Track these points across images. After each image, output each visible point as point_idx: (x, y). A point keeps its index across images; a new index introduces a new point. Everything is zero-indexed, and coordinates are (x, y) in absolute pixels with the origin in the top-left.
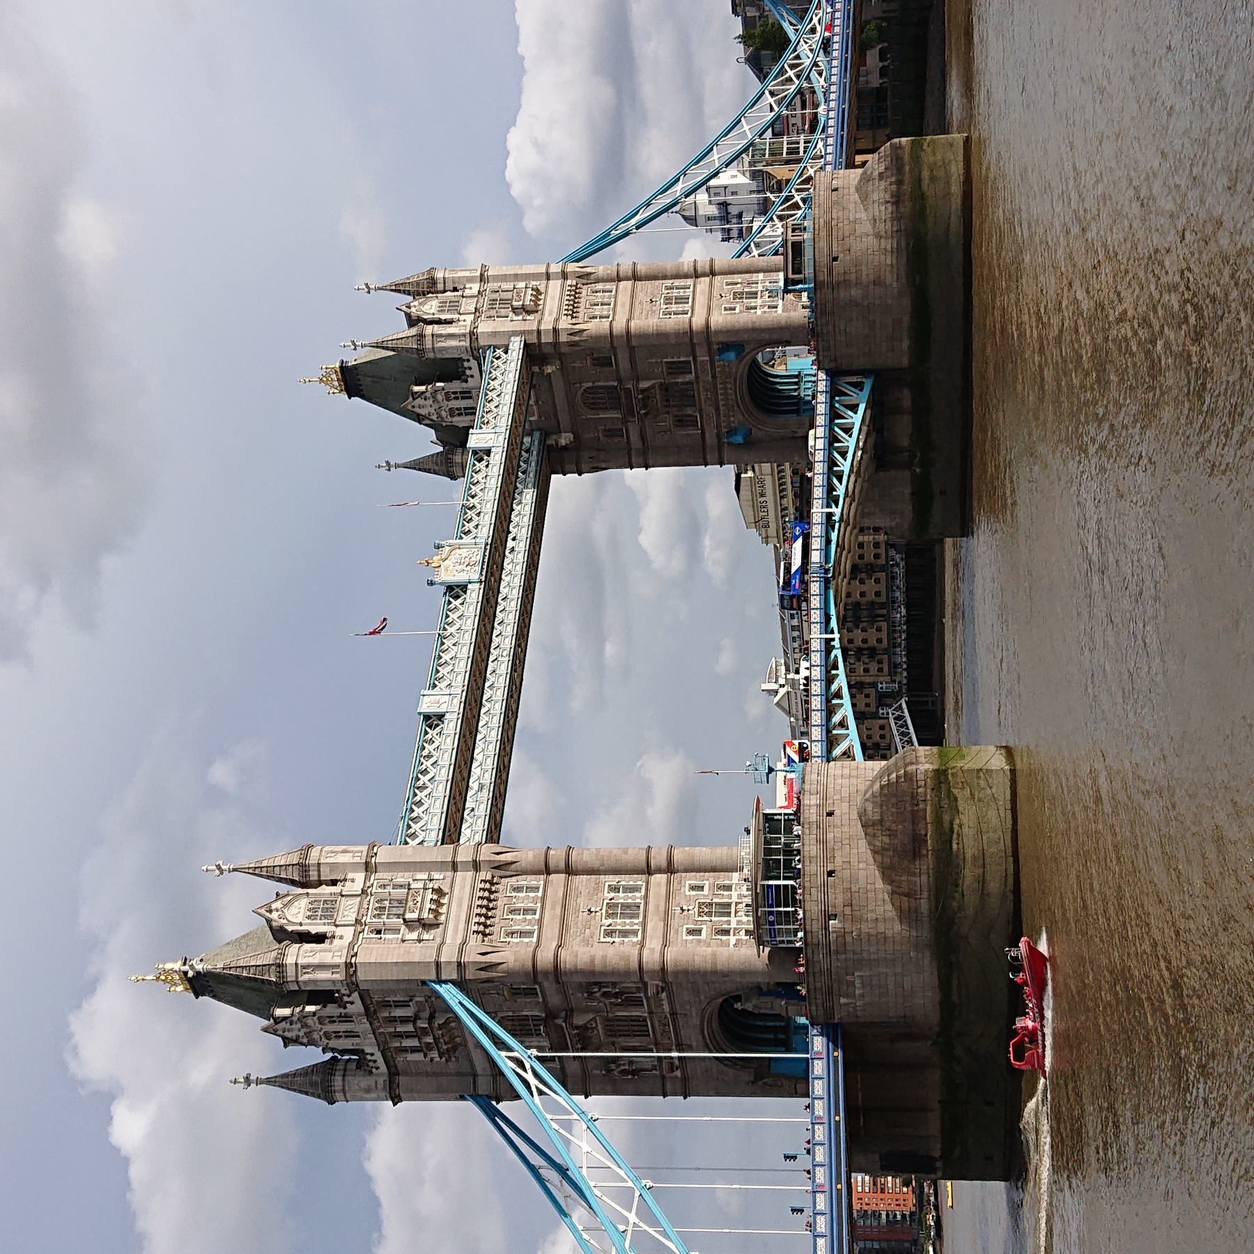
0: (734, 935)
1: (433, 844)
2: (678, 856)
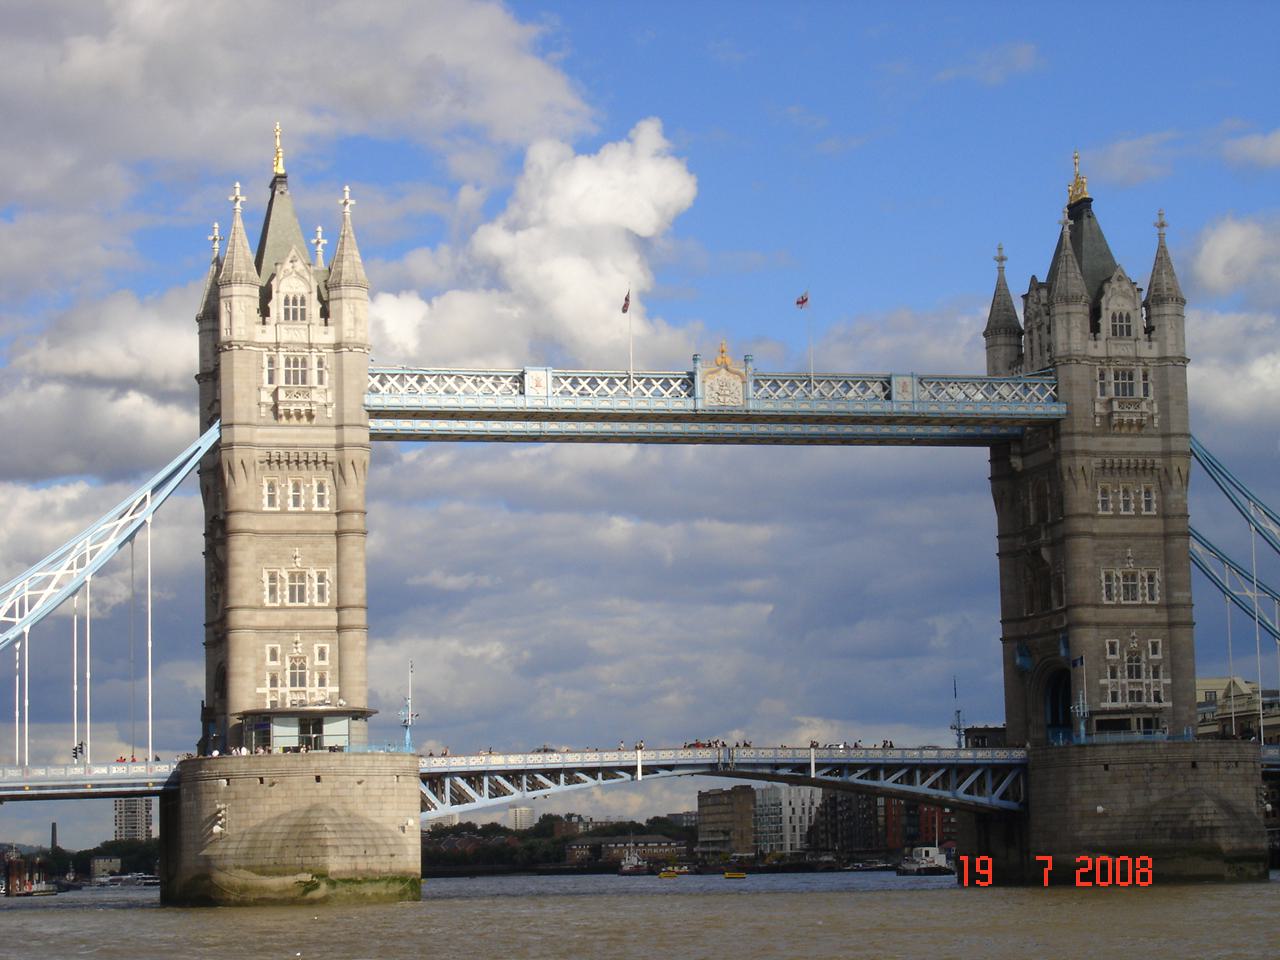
0: (271, 691)
1: (366, 402)
2: (350, 636)
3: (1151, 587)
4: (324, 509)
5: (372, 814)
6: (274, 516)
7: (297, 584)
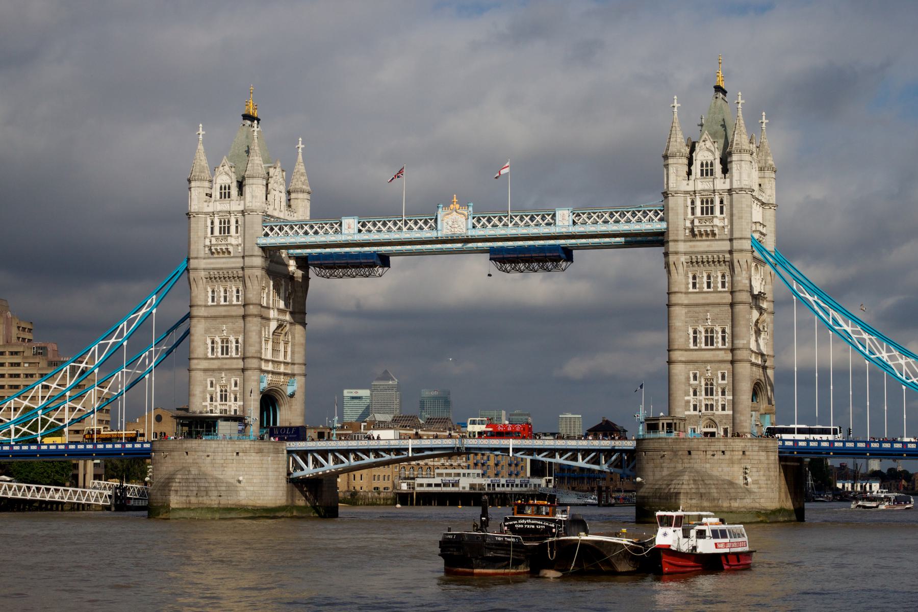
1: (258, 242)
2: (248, 373)
3: (723, 338)
4: (238, 303)
5: (217, 474)
6: (213, 308)
7: (225, 345)
